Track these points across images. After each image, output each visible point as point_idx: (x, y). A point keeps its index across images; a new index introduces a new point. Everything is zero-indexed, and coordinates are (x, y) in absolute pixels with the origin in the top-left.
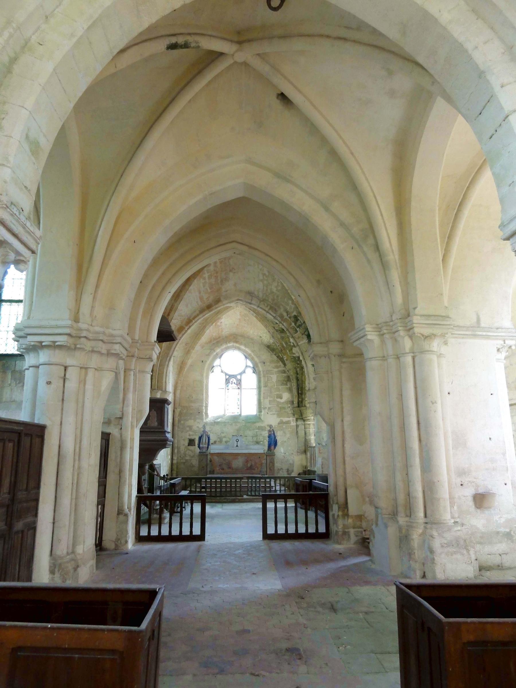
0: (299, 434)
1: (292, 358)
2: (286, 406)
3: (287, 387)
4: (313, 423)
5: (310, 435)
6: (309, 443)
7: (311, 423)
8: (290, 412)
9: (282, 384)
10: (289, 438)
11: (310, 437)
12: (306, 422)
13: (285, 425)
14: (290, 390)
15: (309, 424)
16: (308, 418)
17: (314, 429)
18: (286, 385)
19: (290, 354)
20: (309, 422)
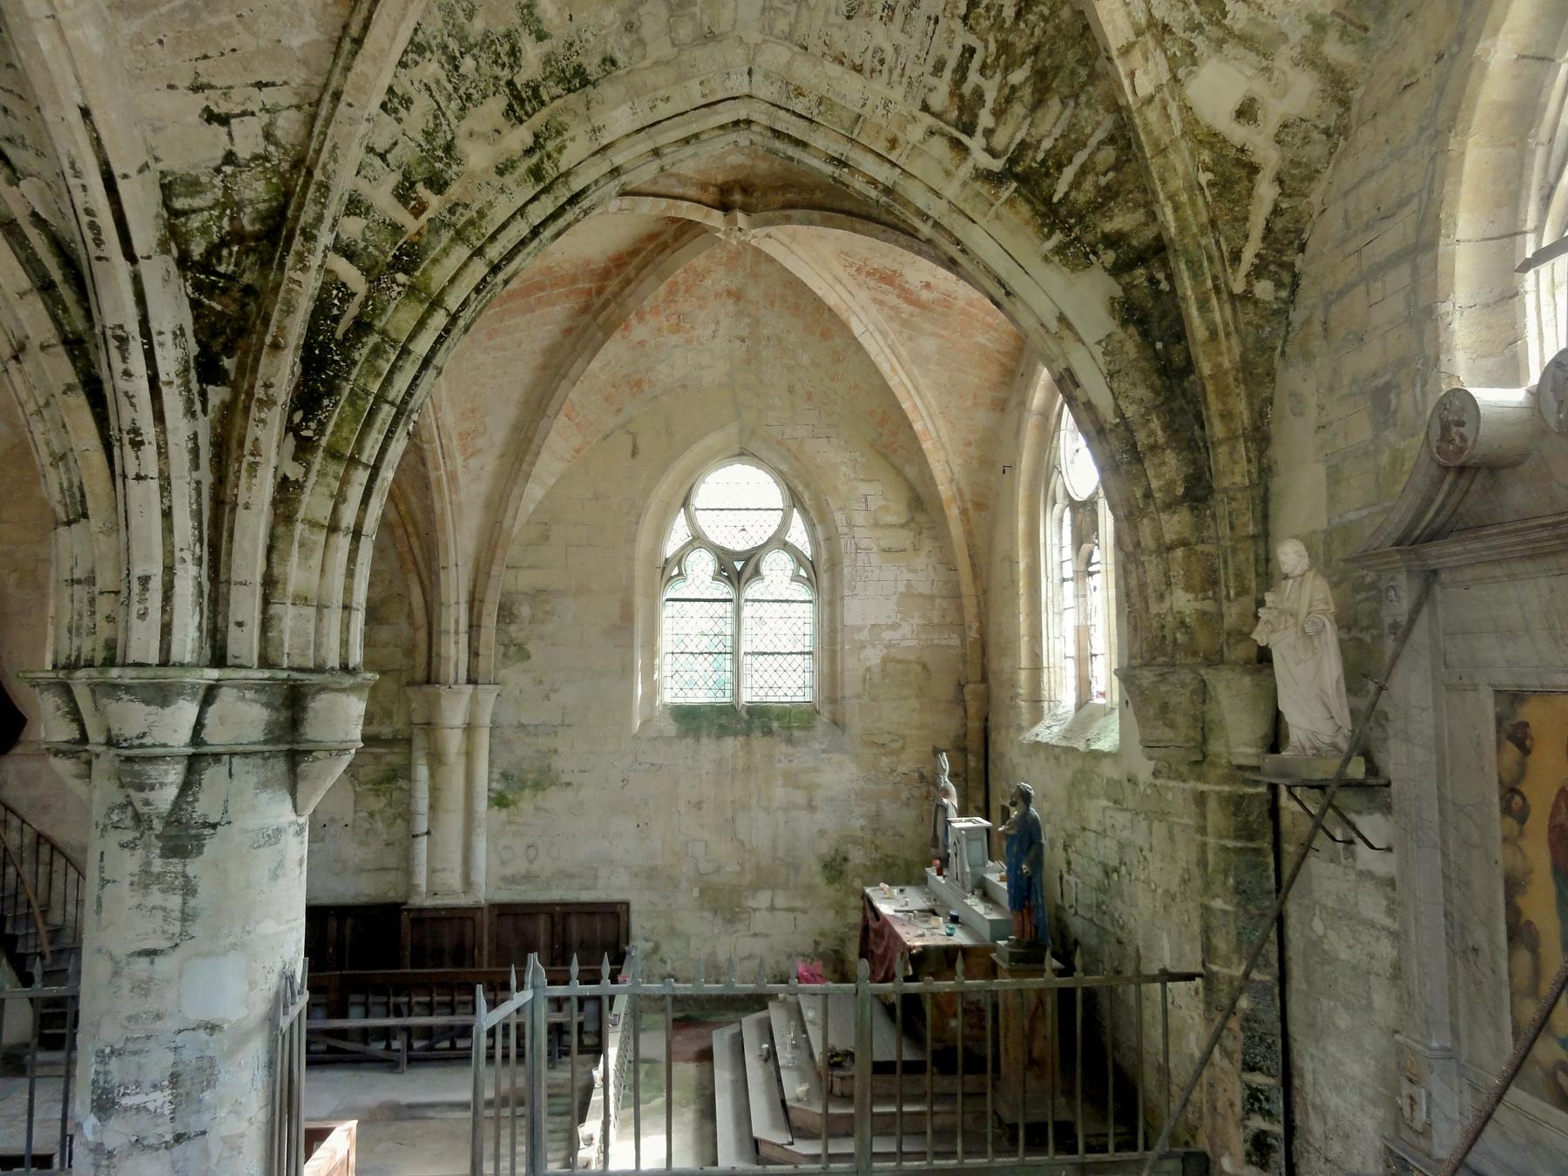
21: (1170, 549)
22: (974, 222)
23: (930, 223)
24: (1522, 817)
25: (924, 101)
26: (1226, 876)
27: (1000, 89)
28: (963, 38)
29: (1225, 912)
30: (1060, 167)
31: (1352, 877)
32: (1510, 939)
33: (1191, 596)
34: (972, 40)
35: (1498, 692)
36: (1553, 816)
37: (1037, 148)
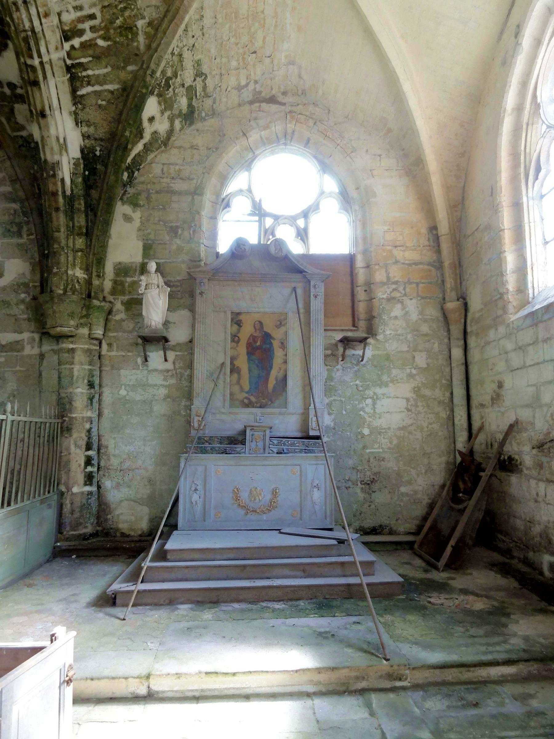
0: (44, 382)
1: (21, 142)
2: (12, 298)
3: (21, 241)
4: (86, 346)
5: (71, 384)
6: (67, 407)
7: (80, 346)
8: (25, 316)
9: (8, 233)
10: (15, 393)
11: (71, 390)
12: (62, 343)
13: (5, 354)
14: (23, 250)
15: (73, 350)
16: (59, 329)
17: (90, 365)
18: (20, 235)
19: (14, 130)
20: (72, 342)
21: (77, 251)
22: (54, 76)
23: (40, 60)
24: (238, 342)
25: (61, 11)
26: (84, 380)
27: (90, 40)
28: (96, 11)
29: (82, 393)
30: (89, 84)
31: (146, 372)
32: (231, 372)
33: (82, 272)
34: (99, 15)
35: (232, 313)
36: (248, 340)
37: (85, 70)
